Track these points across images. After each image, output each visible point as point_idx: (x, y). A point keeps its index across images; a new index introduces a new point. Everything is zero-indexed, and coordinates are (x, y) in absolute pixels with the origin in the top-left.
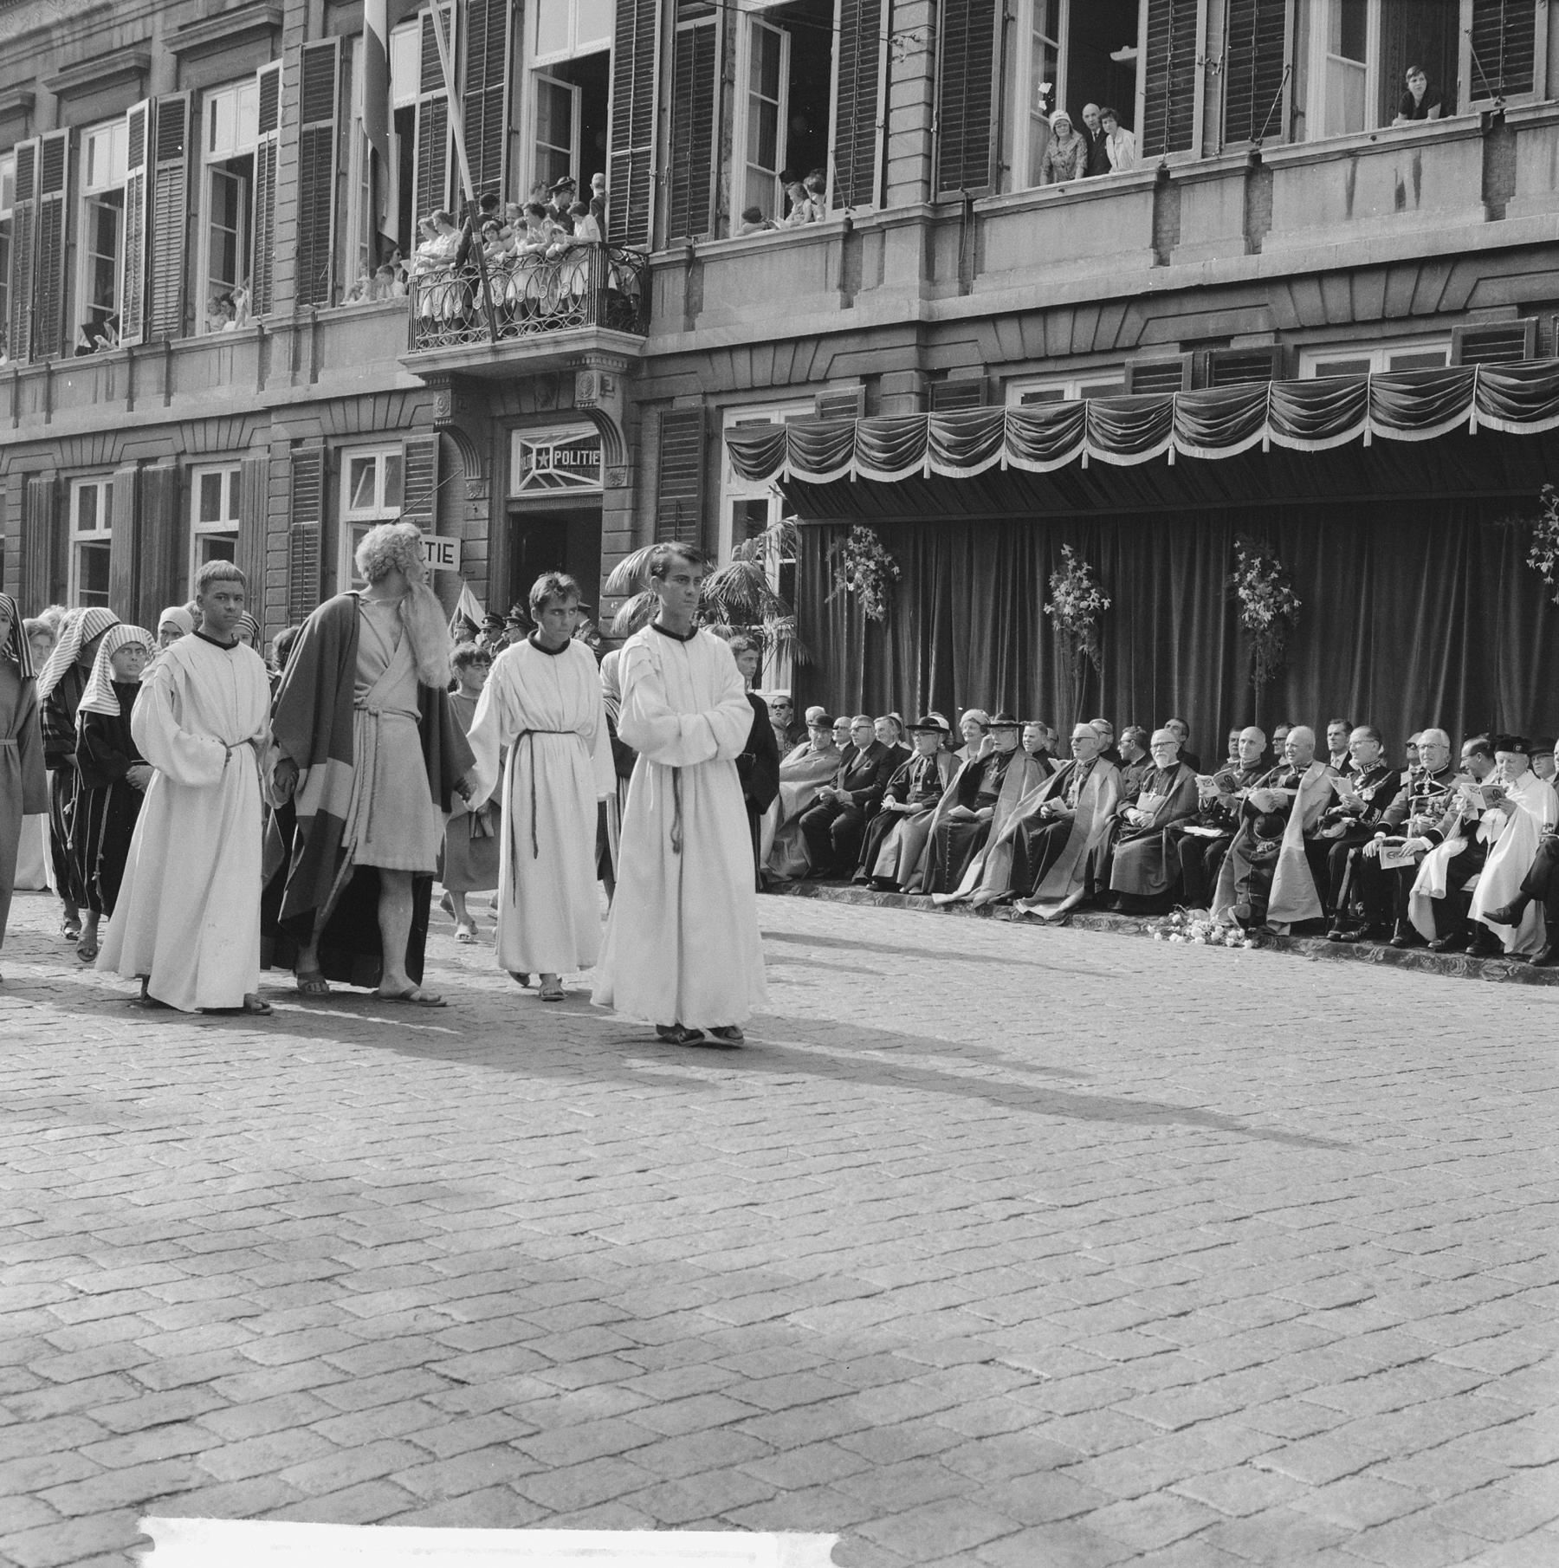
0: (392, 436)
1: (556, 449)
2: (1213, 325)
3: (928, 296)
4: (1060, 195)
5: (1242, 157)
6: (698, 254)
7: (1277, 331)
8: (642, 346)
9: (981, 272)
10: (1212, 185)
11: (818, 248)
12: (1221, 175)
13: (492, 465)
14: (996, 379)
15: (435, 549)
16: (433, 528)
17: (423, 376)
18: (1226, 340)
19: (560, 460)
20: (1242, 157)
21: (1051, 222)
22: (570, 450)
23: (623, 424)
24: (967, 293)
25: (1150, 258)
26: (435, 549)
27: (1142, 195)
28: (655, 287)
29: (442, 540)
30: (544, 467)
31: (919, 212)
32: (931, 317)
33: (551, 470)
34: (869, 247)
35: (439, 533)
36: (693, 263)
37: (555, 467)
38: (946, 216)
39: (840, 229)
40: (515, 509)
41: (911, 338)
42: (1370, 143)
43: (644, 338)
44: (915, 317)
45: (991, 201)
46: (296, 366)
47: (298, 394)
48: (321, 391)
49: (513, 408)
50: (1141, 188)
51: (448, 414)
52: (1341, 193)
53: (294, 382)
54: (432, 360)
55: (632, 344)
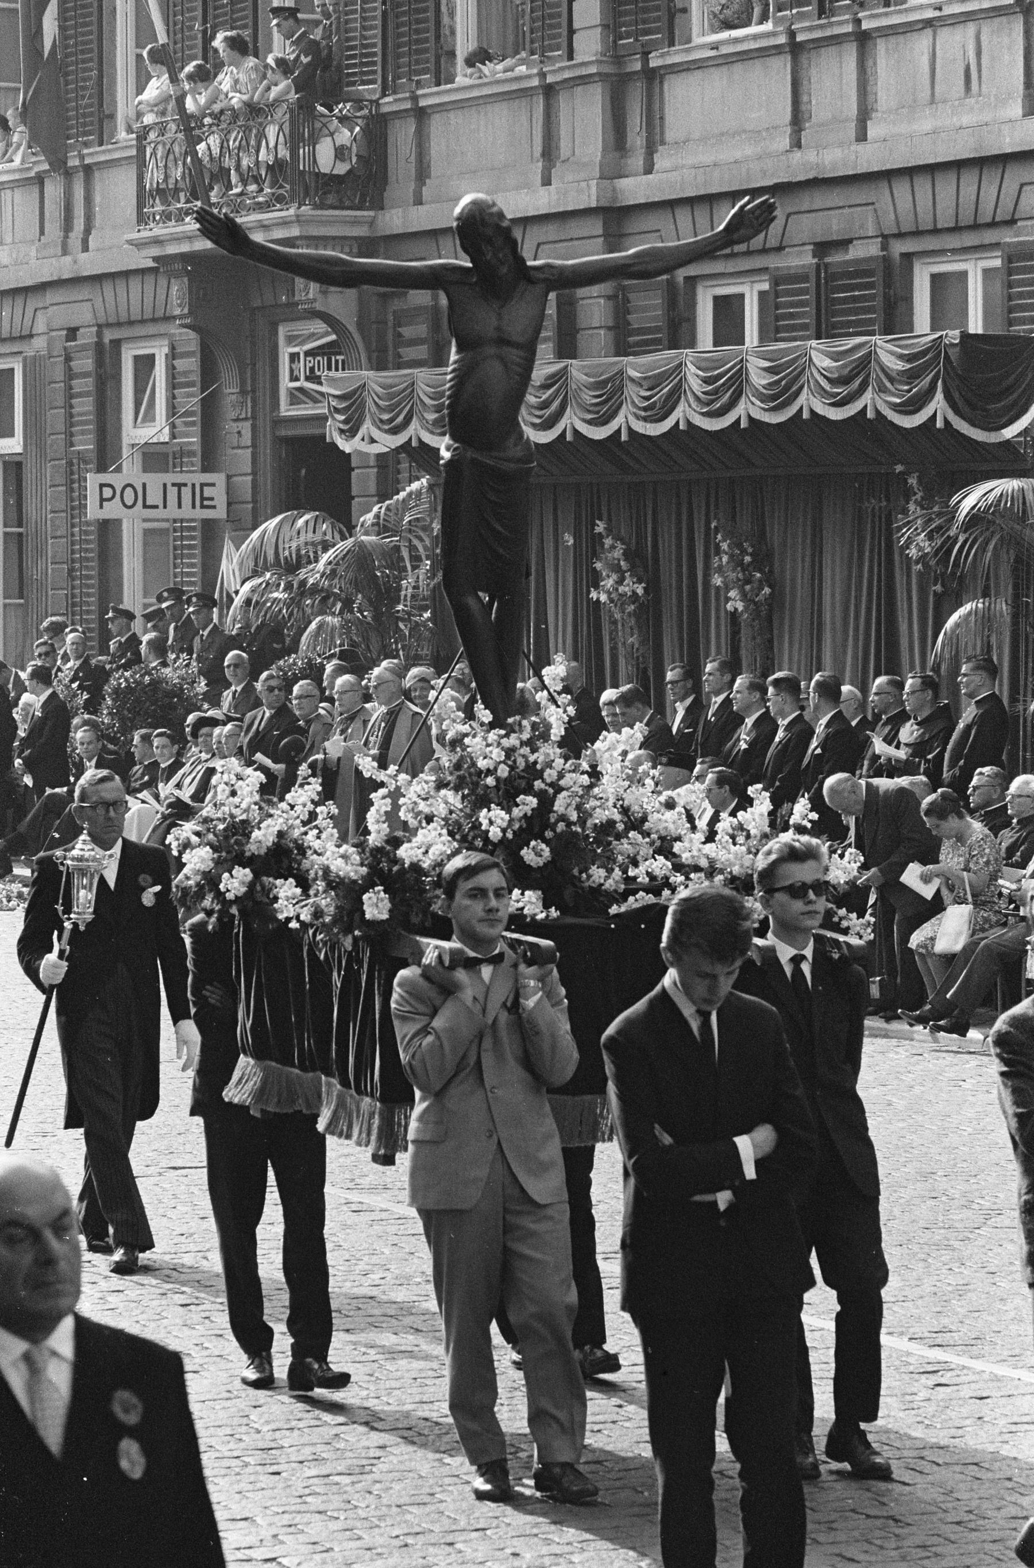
0: (151, 329)
1: (307, 354)
2: (834, 226)
3: (611, 172)
4: (713, 53)
5: (846, 21)
6: (422, 103)
7: (885, 237)
8: (372, 223)
9: (663, 143)
10: (832, 50)
11: (524, 102)
12: (836, 40)
13: (254, 373)
14: (680, 279)
15: (186, 492)
16: (197, 460)
17: (155, 259)
18: (844, 244)
19: (312, 369)
20: (846, 21)
21: (716, 81)
22: (323, 354)
23: (360, 326)
24: (650, 172)
25: (784, 142)
26: (186, 492)
27: (782, 57)
28: (391, 140)
29: (208, 478)
30: (297, 379)
31: (593, 70)
32: (615, 199)
33: (302, 383)
34: (563, 102)
35: (205, 469)
36: (421, 114)
37: (307, 379)
38: (628, 70)
39: (535, 82)
40: (283, 432)
41: (595, 227)
42: (937, 14)
43: (372, 213)
44: (594, 205)
45: (662, 55)
46: (68, 226)
47: (64, 267)
48: (90, 264)
49: (269, 298)
50: (778, 49)
51: (186, 311)
52: (926, 69)
53: (65, 252)
54: (157, 241)
55: (355, 222)
